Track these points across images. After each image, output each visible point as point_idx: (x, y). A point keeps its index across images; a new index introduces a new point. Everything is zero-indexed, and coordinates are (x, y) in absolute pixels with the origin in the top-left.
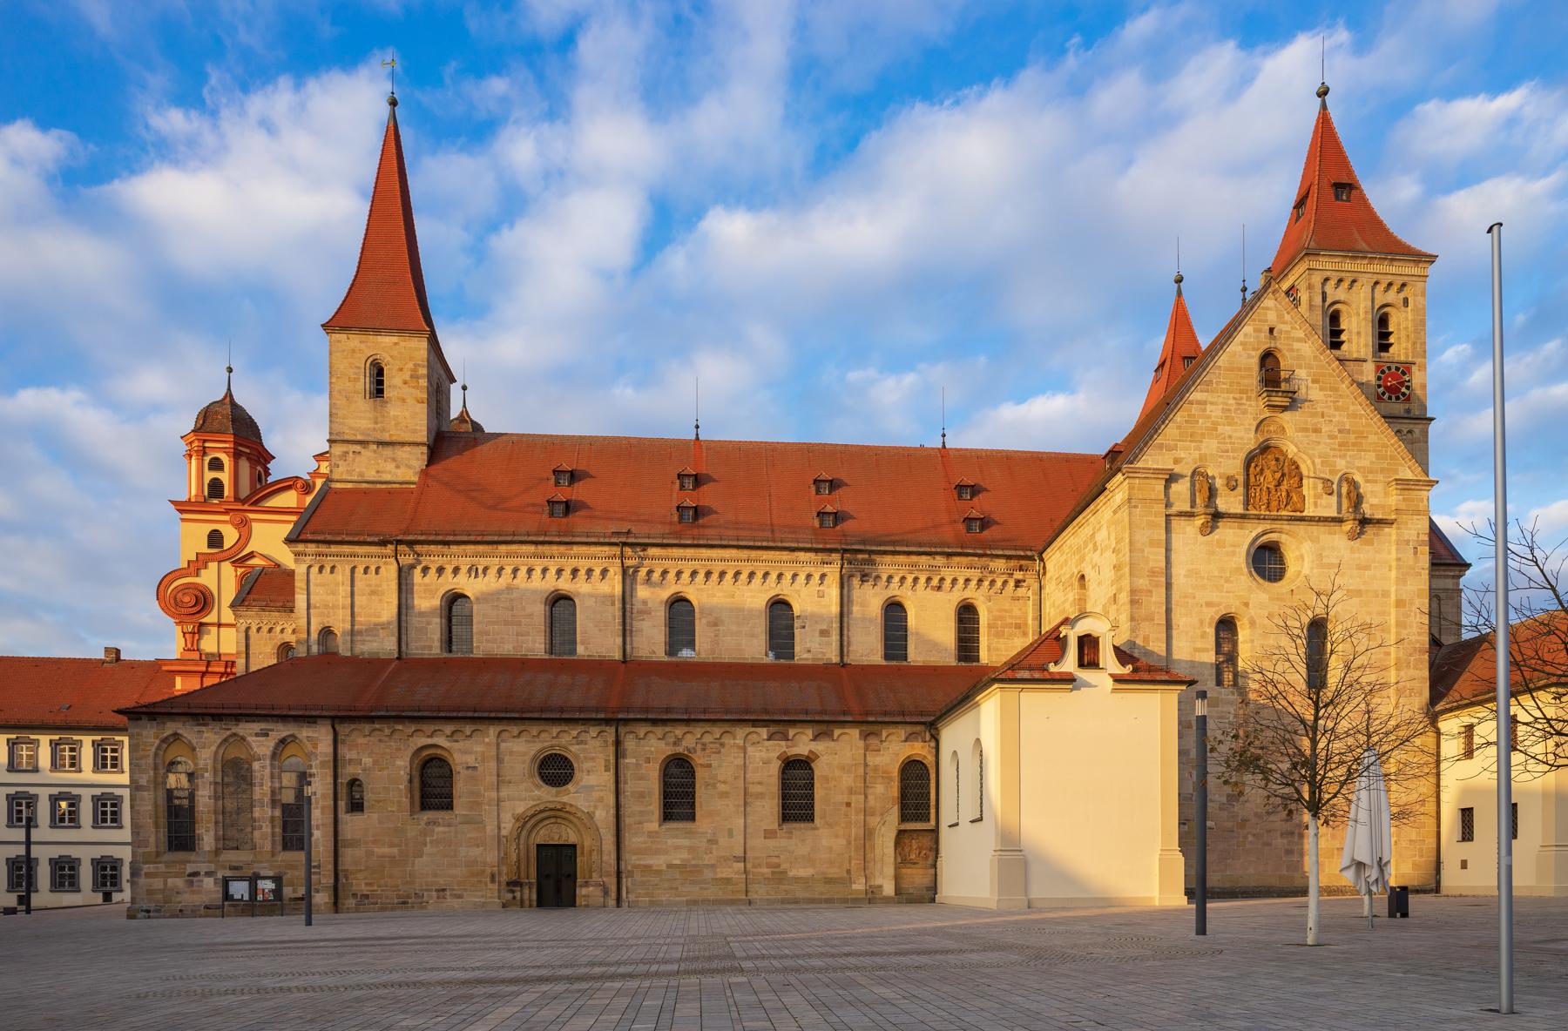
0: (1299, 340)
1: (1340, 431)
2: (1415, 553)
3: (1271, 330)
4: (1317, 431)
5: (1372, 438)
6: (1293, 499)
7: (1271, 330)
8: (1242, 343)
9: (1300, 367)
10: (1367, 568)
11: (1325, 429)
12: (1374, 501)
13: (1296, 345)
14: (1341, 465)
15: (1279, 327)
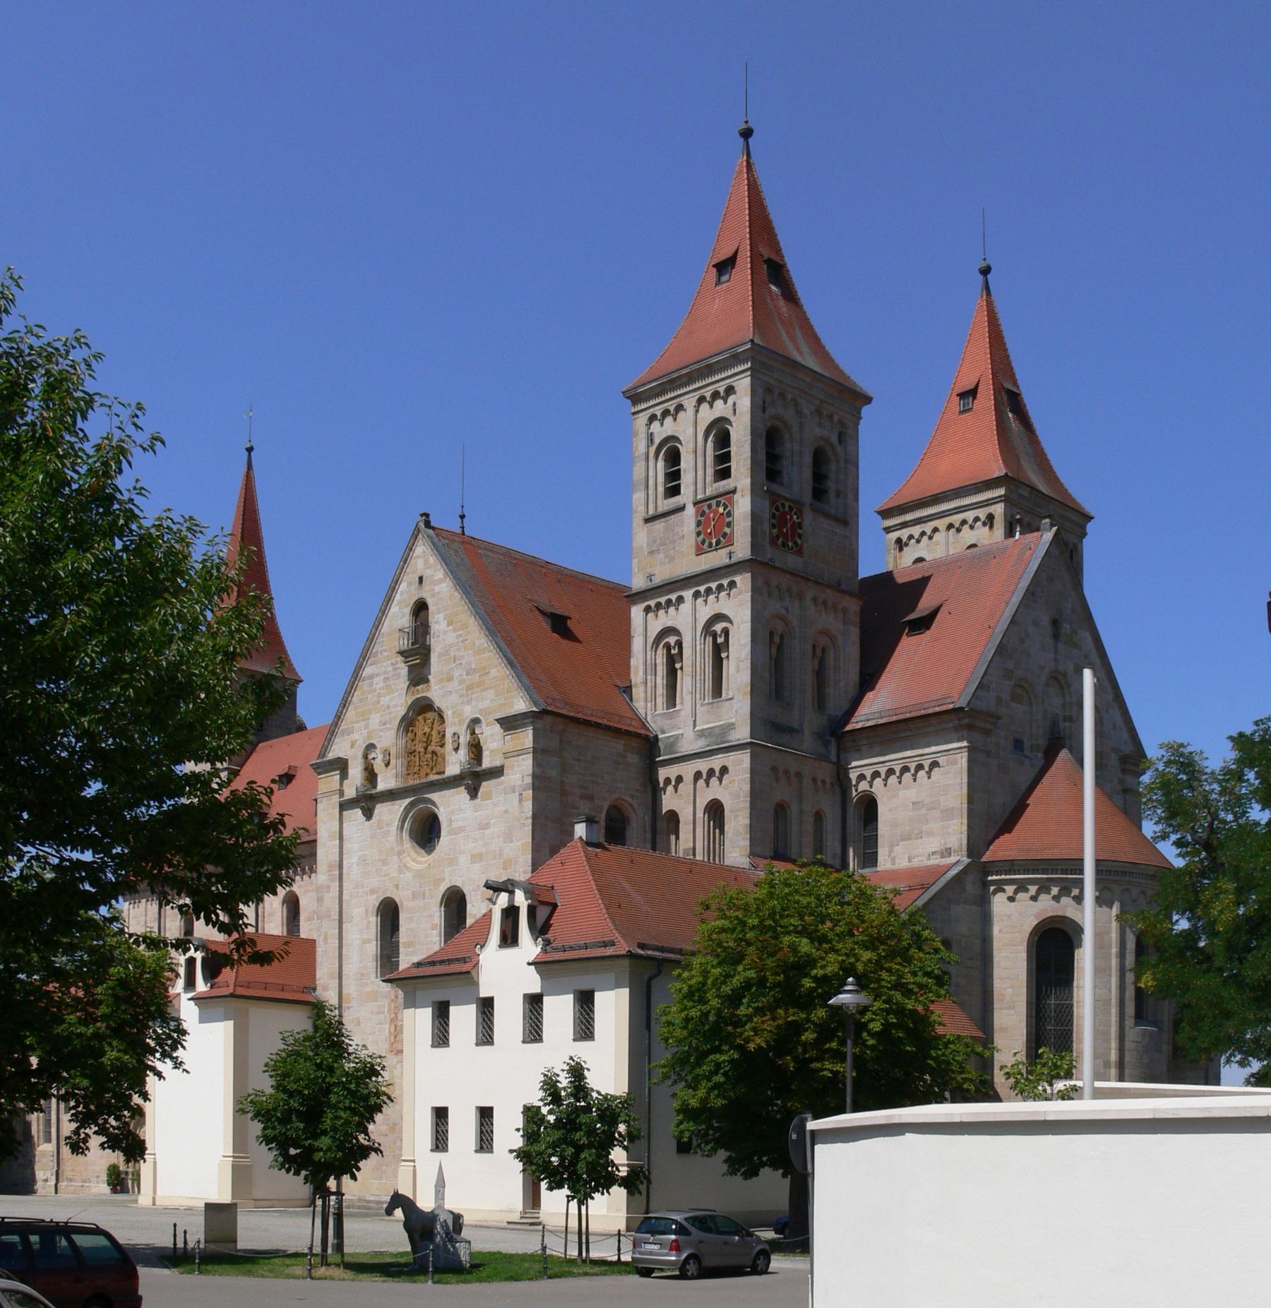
0: (440, 581)
1: (468, 674)
2: (521, 801)
3: (421, 579)
4: (450, 679)
5: (494, 672)
6: (436, 759)
7: (421, 579)
8: (399, 603)
9: (439, 613)
10: (487, 826)
11: (456, 675)
12: (494, 745)
13: (437, 589)
14: (469, 712)
15: (427, 574)
